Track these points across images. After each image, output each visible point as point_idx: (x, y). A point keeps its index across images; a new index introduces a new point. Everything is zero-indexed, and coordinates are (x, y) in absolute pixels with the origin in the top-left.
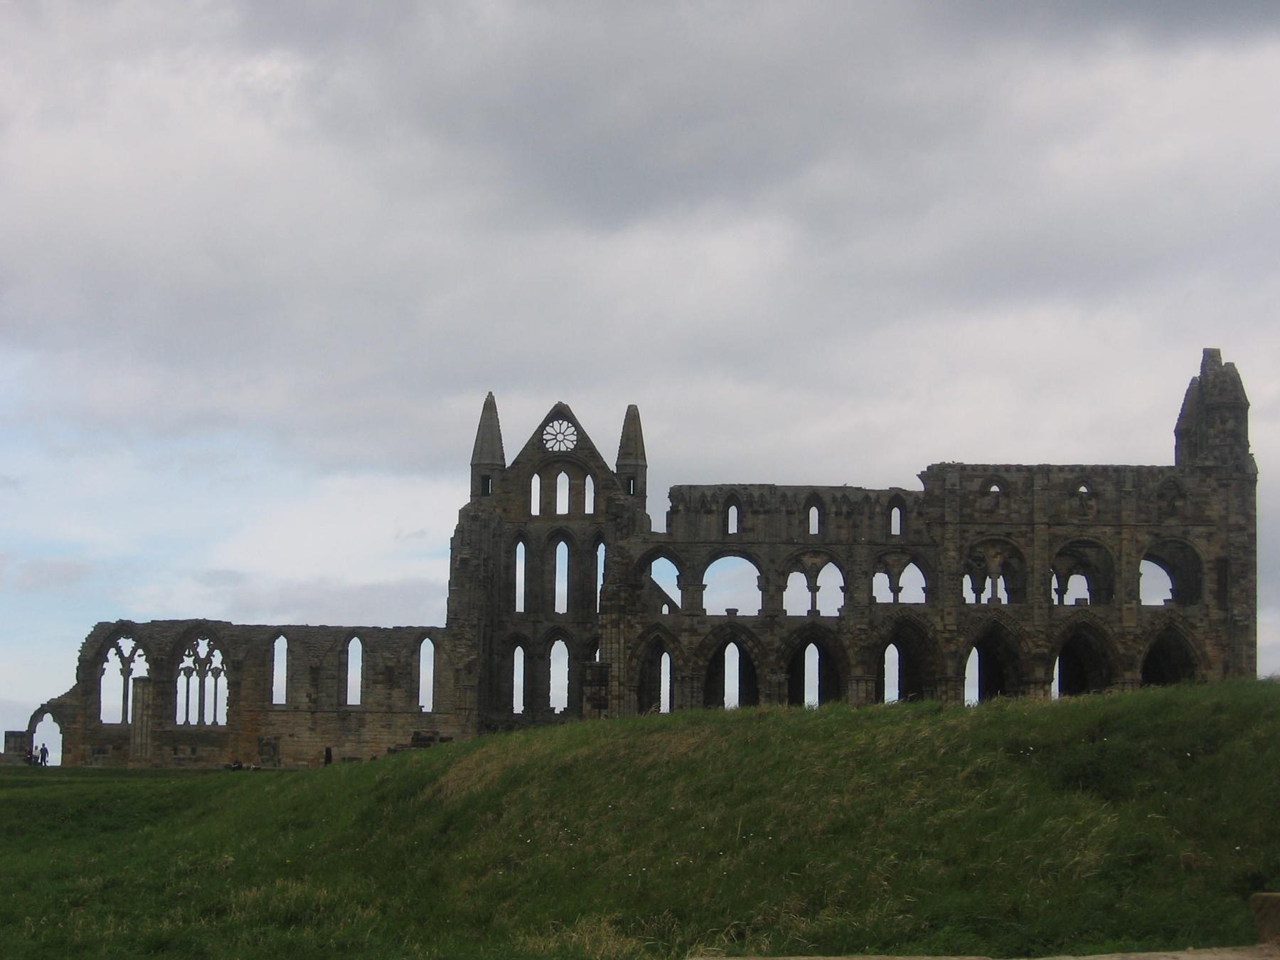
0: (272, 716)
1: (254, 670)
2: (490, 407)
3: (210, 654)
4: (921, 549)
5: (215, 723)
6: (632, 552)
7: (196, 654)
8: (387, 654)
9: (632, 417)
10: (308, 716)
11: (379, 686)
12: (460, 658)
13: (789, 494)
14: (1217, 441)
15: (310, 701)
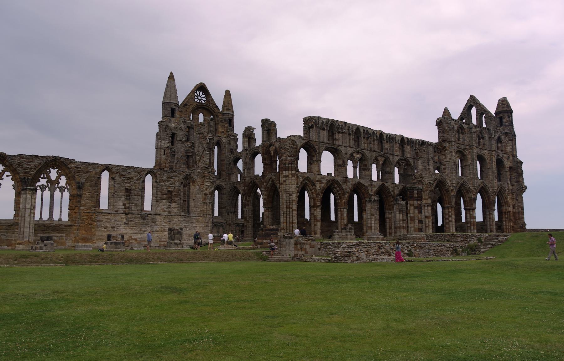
0: (101, 216)
1: (91, 188)
2: (171, 77)
3: (58, 178)
4: (389, 156)
5: (60, 219)
6: (298, 143)
7: (49, 177)
8: (168, 184)
9: (228, 94)
10: (124, 216)
11: (164, 201)
12: (207, 189)
13: (351, 126)
14: (507, 124)
15: (125, 208)
